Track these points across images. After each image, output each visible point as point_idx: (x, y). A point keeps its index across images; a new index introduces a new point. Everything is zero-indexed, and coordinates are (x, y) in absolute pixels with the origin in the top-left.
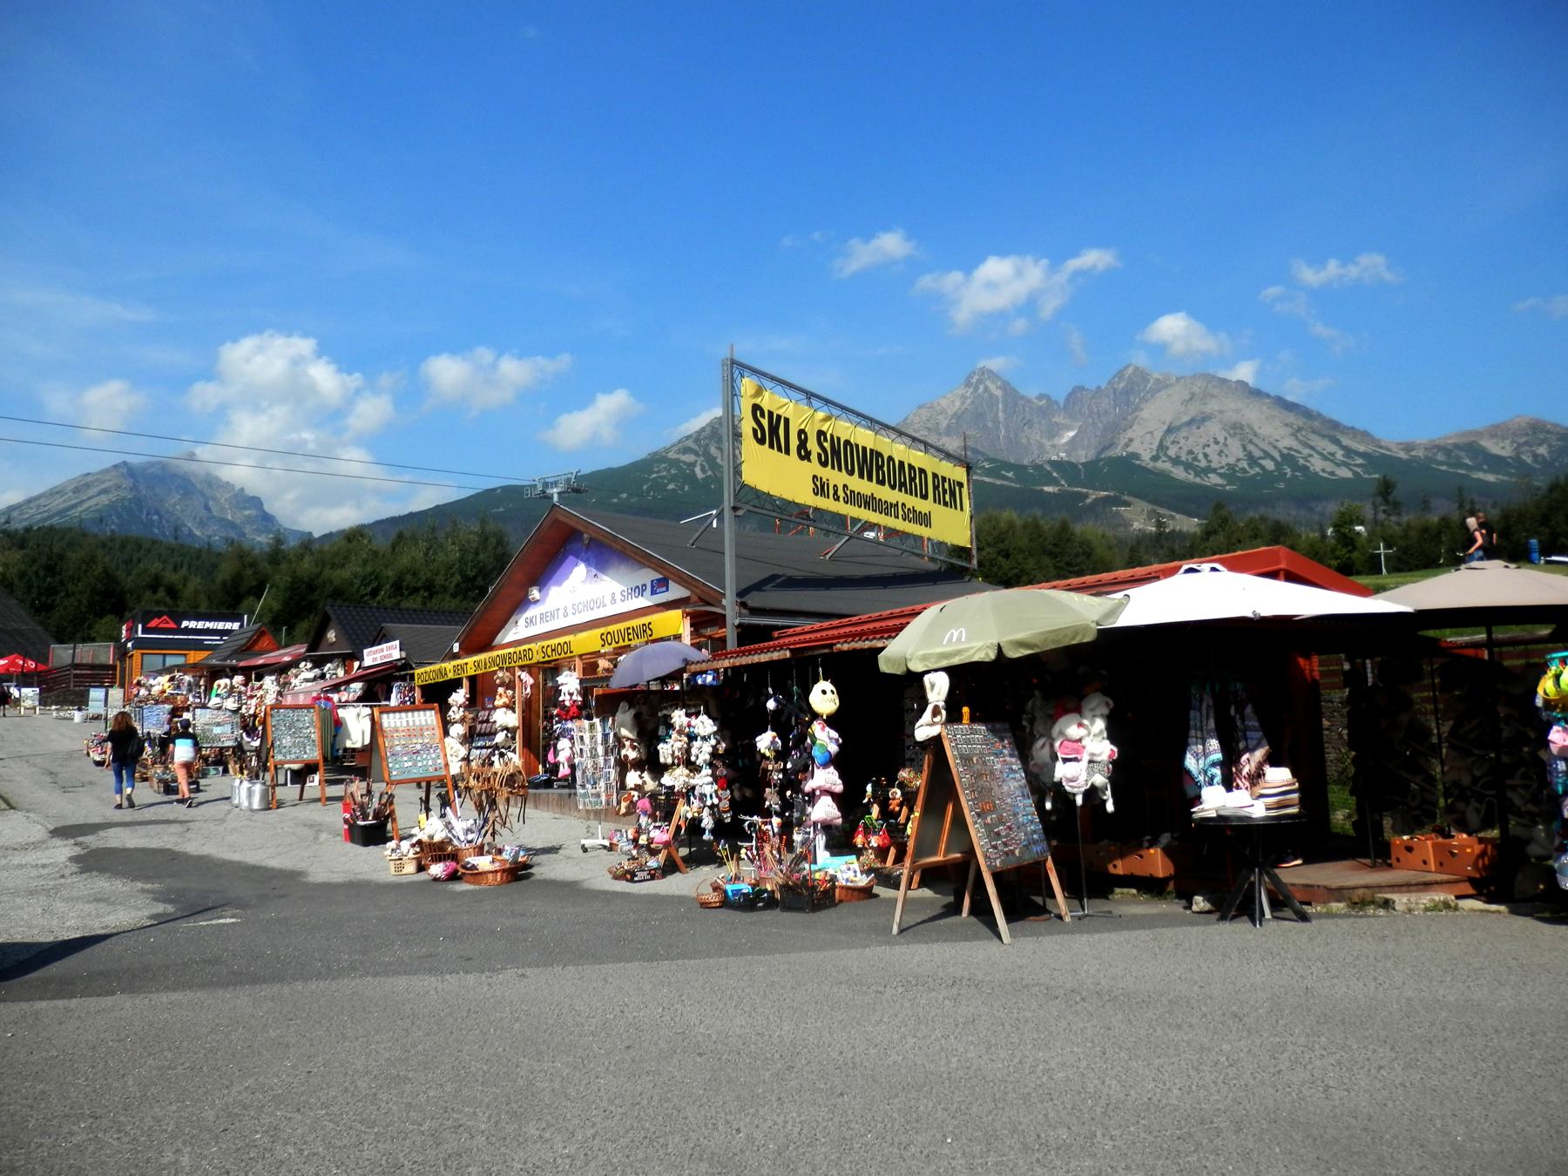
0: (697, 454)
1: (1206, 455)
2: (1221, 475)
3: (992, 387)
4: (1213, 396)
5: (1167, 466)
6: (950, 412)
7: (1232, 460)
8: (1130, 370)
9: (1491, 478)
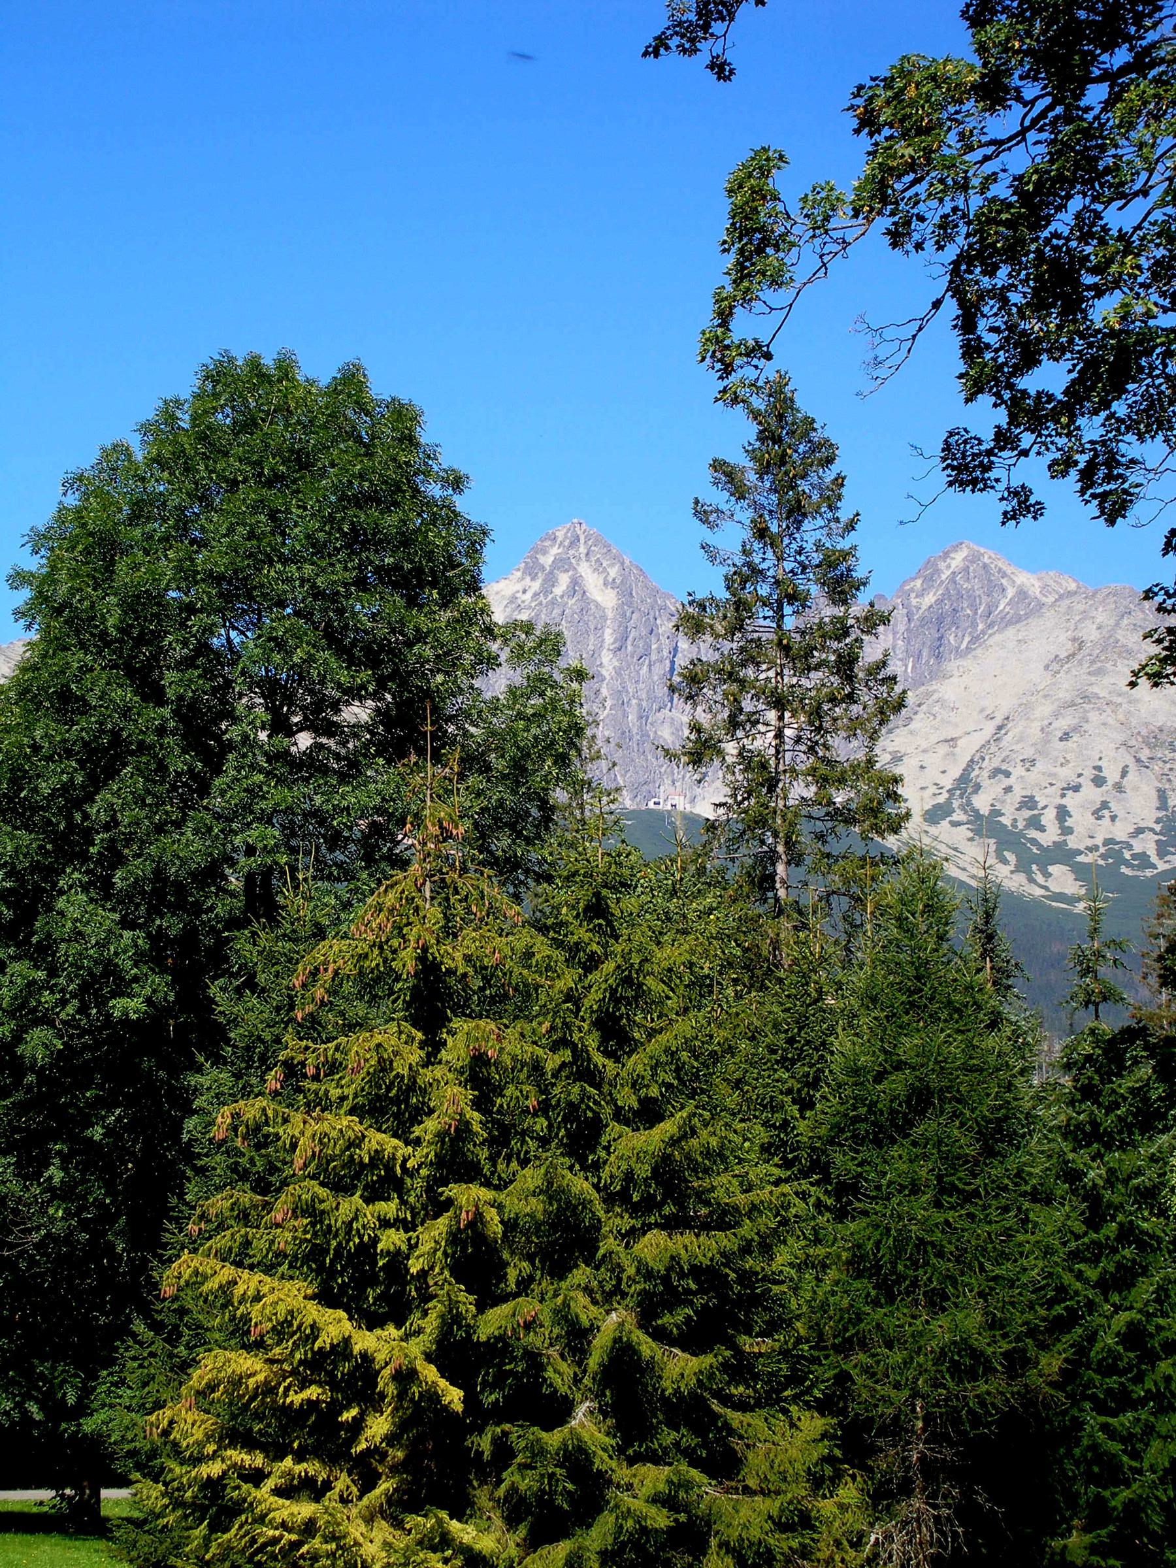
1: (1063, 813)
7: (1120, 832)
8: (958, 559)
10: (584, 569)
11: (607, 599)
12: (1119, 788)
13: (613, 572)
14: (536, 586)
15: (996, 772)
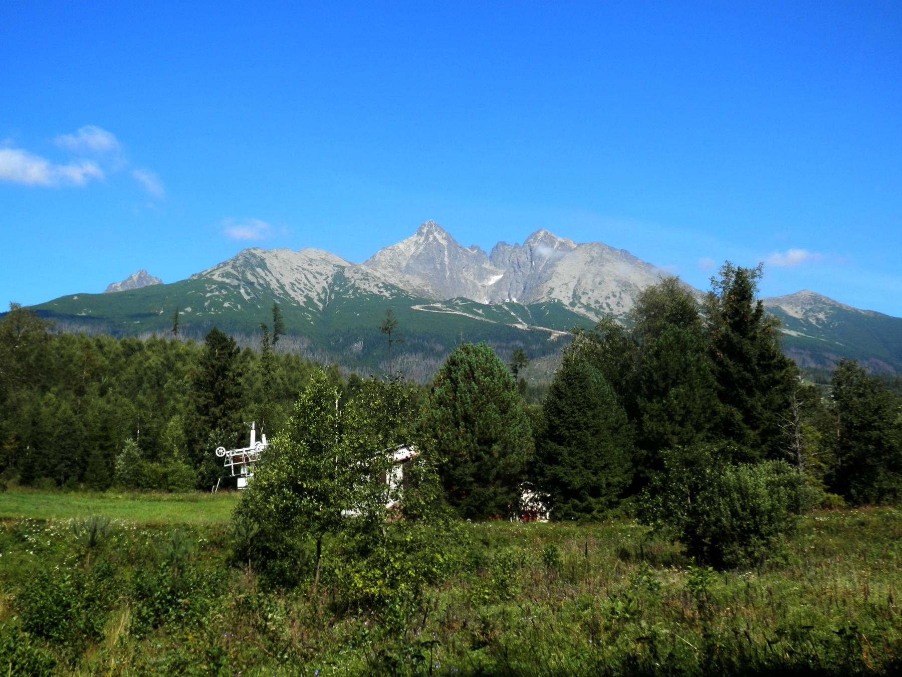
0: (238, 280)
1: (608, 305)
2: (620, 320)
3: (438, 236)
4: (608, 260)
5: (582, 311)
6: (408, 255)
9: (793, 333)
10: (435, 234)
11: (444, 243)
12: (620, 298)
13: (444, 235)
14: (423, 238)
15: (584, 293)
